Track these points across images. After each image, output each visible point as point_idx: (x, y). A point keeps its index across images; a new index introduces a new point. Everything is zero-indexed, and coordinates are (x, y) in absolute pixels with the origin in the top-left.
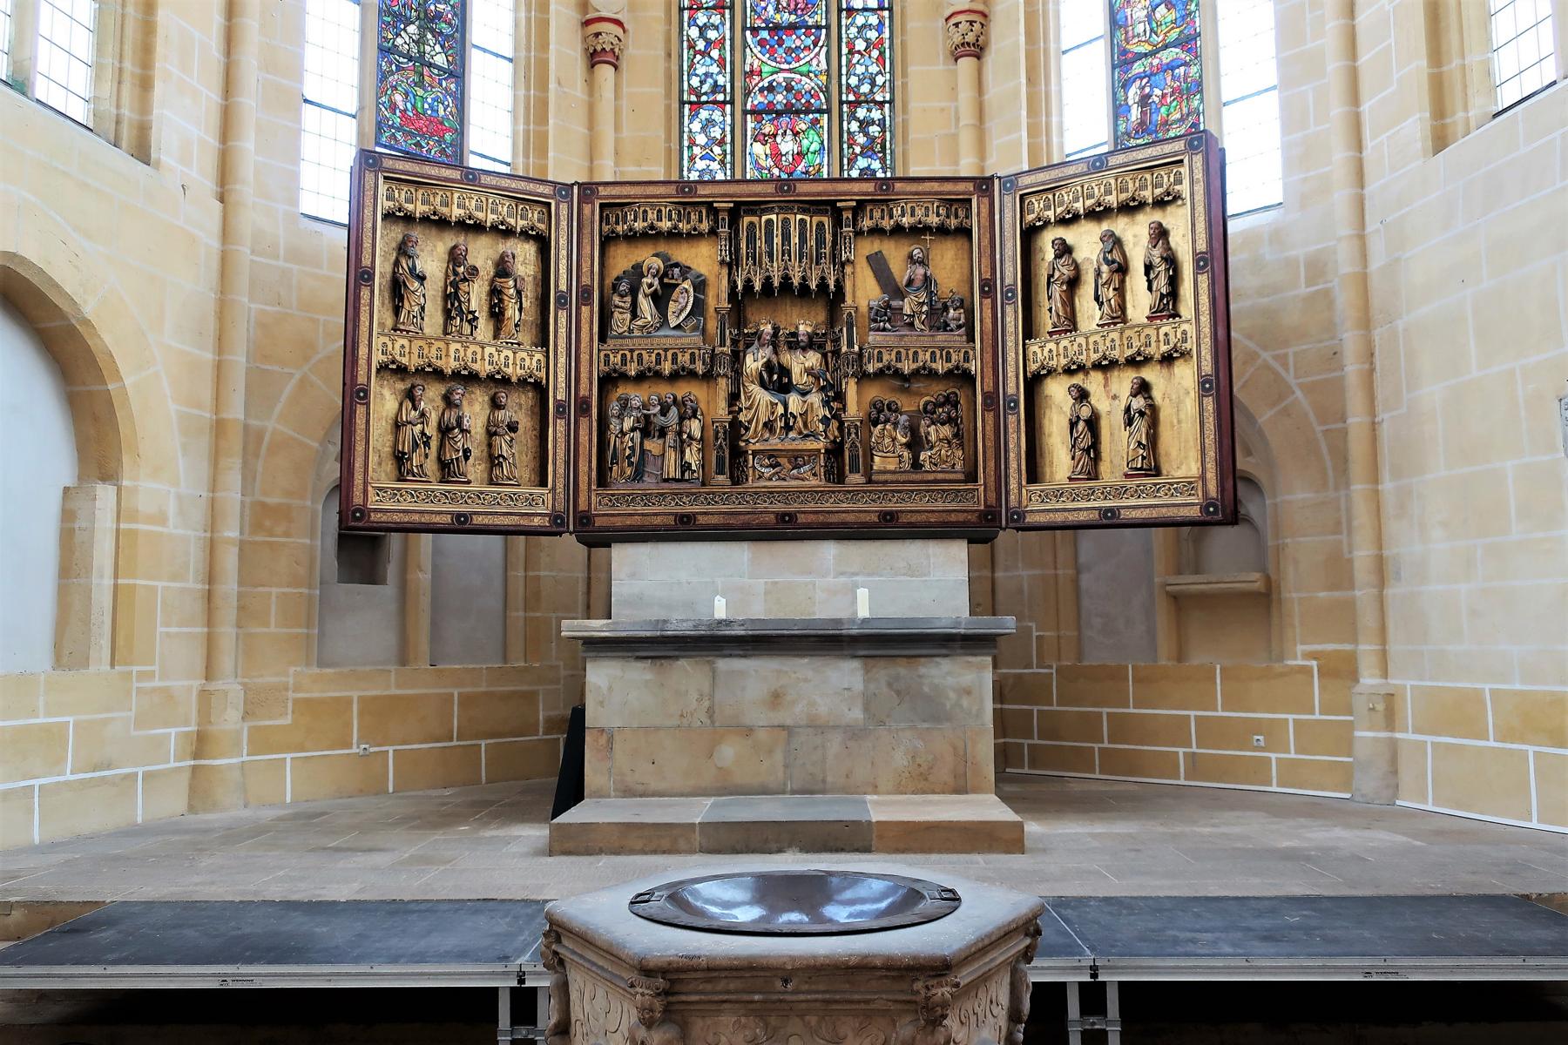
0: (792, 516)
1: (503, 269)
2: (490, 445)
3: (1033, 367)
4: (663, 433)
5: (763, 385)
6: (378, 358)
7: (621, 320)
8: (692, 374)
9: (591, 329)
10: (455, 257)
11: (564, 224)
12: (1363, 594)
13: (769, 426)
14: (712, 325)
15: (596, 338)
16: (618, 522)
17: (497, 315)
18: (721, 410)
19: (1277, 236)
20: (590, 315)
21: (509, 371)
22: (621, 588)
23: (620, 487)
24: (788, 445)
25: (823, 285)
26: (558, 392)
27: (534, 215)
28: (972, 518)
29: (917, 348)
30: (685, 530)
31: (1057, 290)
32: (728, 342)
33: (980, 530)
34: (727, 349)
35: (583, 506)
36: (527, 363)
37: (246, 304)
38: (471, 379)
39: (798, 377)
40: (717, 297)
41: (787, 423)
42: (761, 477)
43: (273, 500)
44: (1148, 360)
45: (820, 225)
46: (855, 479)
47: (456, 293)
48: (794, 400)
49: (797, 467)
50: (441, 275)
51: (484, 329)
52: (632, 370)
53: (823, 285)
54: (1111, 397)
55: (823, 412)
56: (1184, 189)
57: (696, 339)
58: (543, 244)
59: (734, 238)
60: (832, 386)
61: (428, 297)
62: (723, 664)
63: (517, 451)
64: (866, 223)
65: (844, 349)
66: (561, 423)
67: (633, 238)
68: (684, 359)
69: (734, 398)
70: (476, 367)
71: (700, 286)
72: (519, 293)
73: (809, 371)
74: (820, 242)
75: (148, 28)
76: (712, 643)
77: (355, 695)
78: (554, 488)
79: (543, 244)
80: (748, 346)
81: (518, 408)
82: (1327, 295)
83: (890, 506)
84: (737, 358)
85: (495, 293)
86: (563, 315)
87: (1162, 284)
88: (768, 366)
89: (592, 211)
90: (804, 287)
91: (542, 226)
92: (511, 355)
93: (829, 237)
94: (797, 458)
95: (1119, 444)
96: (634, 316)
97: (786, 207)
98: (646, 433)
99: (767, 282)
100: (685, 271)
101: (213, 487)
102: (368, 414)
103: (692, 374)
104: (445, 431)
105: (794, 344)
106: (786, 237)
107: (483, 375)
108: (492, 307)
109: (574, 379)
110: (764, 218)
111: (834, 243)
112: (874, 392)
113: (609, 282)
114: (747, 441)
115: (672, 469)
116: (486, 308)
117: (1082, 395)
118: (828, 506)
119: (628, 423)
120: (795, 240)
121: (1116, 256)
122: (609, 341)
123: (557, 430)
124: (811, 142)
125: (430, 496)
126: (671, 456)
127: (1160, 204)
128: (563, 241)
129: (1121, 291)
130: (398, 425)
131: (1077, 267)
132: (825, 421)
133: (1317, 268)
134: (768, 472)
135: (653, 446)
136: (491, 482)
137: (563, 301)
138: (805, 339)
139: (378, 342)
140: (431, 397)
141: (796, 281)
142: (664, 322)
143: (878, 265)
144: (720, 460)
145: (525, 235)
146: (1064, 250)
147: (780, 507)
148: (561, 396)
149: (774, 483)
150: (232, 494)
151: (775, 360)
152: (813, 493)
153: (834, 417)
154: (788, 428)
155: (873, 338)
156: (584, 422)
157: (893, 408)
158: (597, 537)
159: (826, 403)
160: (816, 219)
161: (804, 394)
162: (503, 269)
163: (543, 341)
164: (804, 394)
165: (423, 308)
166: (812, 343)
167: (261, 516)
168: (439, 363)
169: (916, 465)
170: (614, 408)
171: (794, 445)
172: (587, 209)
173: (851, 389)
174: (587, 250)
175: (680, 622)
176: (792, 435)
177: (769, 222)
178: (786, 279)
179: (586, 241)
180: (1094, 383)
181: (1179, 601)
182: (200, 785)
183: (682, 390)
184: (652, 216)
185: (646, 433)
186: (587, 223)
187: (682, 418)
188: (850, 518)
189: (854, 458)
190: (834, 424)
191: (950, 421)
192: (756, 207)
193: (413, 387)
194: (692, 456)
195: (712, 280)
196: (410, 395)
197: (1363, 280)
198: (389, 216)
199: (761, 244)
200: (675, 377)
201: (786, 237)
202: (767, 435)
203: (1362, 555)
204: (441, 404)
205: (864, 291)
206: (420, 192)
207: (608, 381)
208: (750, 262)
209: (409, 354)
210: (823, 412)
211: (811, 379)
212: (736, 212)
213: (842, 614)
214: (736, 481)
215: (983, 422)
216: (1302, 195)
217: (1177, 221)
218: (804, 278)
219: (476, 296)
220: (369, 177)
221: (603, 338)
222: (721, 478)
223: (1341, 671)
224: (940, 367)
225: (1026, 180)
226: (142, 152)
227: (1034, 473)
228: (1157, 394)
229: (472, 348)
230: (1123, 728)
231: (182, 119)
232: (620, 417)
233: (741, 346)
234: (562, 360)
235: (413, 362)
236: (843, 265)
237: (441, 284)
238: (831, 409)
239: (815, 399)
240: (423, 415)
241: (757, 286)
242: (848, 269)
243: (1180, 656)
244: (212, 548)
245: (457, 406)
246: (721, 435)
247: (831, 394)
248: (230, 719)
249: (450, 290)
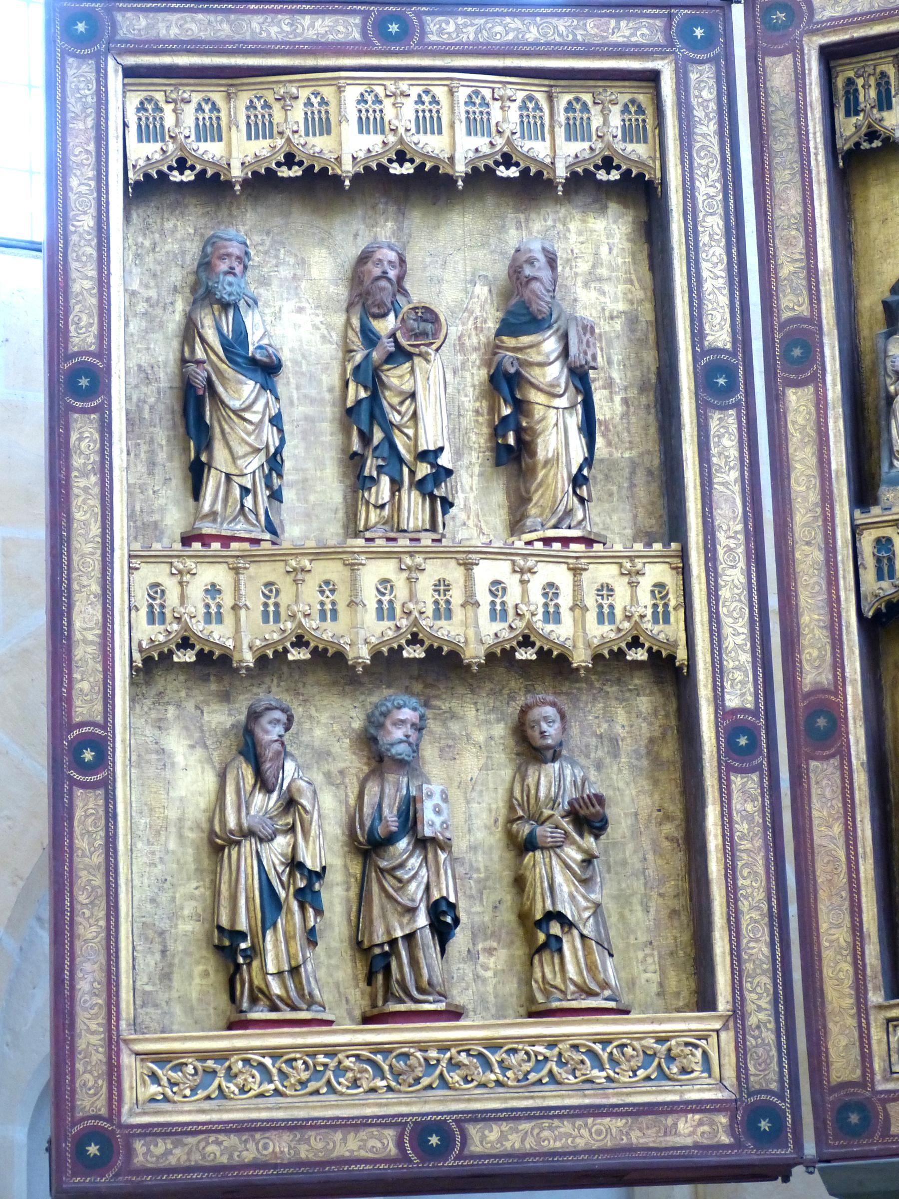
1: (522, 314)
2: (519, 883)
9: (823, 461)
10: (369, 291)
11: (707, 130)
15: (842, 489)
21: (562, 632)
26: (729, 683)
27: (609, 119)
36: (621, 598)
38: (441, 667)
47: (375, 398)
50: (330, 351)
51: (477, 501)
63: (616, 902)
66: (746, 788)
70: (449, 631)
72: (580, 377)
78: (738, 1013)
79: (641, 194)
81: (609, 750)
85: (506, 384)
86: (725, 429)
91: (639, 151)
92: (561, 575)
102: (111, 816)
107: (474, 653)
108: (498, 429)
113: (871, 301)
116: (478, 437)
122: (887, 494)
123: (735, 810)
128: (708, 188)
137: (722, 379)
145: (584, 186)
148: (740, 695)
156: (823, 777)
165: (275, 462)
168: (328, 632)
172: (779, 73)
174: (788, 204)
179: (784, 177)
186: (781, 116)
193: (254, 716)
204: (349, 761)
206: (244, 99)
219: (441, 404)
221: (864, 493)
229: (434, 570)
234: (734, 576)
237: (337, 382)
240: (290, 803)
245: (401, 764)
249: (356, 393)
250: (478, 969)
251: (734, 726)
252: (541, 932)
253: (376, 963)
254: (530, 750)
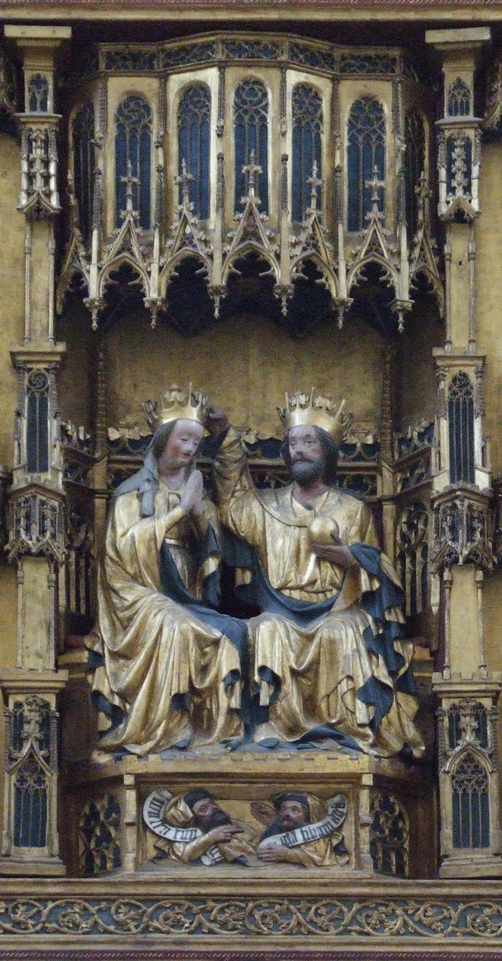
5: (170, 586)
13: (190, 705)
24: (250, 762)
25: (373, 279)
32: (55, 457)
34: (55, 479)
41: (250, 699)
42: (159, 848)
48: (273, 640)
49: (285, 826)
55: (367, 669)
59: (74, 145)
60: (398, 592)
65: (441, 482)
73: (324, 549)
80: (118, 478)
93: (393, 143)
94: (280, 801)
99: (188, 275)
105: (274, 469)
106: (250, 137)
110: (177, 82)
111: (412, 162)
114: (120, 751)
120: (281, 145)
132: (375, 693)
134: (186, 840)
138: (312, 451)
141: (284, 274)
149: (206, 871)
151: (209, 515)
153: (404, 684)
154: (252, 712)
159: (378, 644)
160: (351, 90)
161: (305, 614)
164: (305, 614)
171: (272, 764)
176: (263, 733)
177: (196, 95)
178: (251, 266)
190: (406, 705)
199: (165, 159)
201: (250, 137)
202: (183, 734)
208: (130, 213)
210: (367, 669)
211: (329, 572)
218: (310, 267)
222: (32, 853)
233: (99, 477)
236: (439, 229)
238: (394, 662)
239: (345, 634)
241: (154, 288)
242: (457, 245)
246: (31, 729)
247: (395, 617)
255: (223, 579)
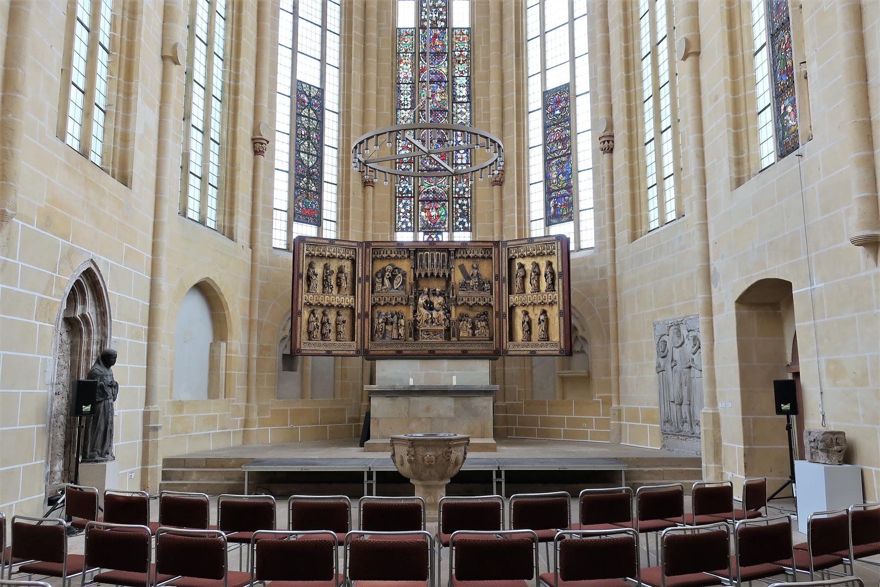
0: (433, 351)
3: (511, 304)
4: (392, 323)
5: (425, 308)
6: (304, 301)
7: (378, 286)
8: (402, 304)
10: (326, 267)
12: (613, 378)
13: (426, 321)
14: (408, 288)
16: (377, 353)
17: (339, 285)
18: (411, 317)
19: (592, 260)
20: (369, 285)
22: (379, 374)
23: (378, 341)
25: (444, 275)
26: (358, 310)
28: (492, 352)
29: (475, 296)
30: (399, 356)
31: (519, 280)
33: (495, 355)
35: (366, 347)
37: (259, 281)
39: (436, 305)
40: (410, 279)
42: (424, 338)
43: (265, 345)
44: (545, 304)
45: (444, 256)
46: (454, 339)
52: (382, 303)
53: (444, 275)
54: (535, 314)
56: (555, 251)
57: (403, 293)
58: (354, 262)
61: (318, 282)
62: (412, 399)
63: (345, 329)
64: (458, 255)
67: (382, 258)
68: (399, 300)
69: (415, 312)
71: (404, 275)
73: (439, 304)
74: (443, 261)
75: (232, 196)
76: (409, 392)
77: (289, 409)
79: (354, 262)
82: (605, 281)
83: (466, 348)
84: (416, 299)
85: (338, 278)
86: (360, 285)
87: (549, 280)
88: (426, 302)
89: (369, 251)
90: (438, 276)
94: (435, 332)
95: (537, 330)
96: (383, 285)
97: (432, 250)
98: (386, 324)
100: (399, 270)
101: (249, 340)
103: (402, 304)
104: (323, 324)
109: (363, 306)
112: (461, 310)
115: (395, 336)
117: (526, 313)
118: (445, 348)
119: (381, 320)
120: (435, 261)
121: (536, 270)
123: (358, 323)
124: (442, 212)
125: (320, 345)
126: (395, 331)
127: (549, 254)
129: (538, 281)
130: (309, 322)
131: (525, 271)
132: (444, 320)
133: (603, 272)
135: (389, 328)
136: (337, 340)
139: (304, 296)
140: (319, 312)
142: (393, 287)
143: (462, 268)
144: (410, 333)
146: (522, 266)
147: (430, 348)
150: (255, 344)
152: (441, 344)
154: (432, 322)
155: (460, 293)
156: (366, 320)
157: (467, 316)
158: (371, 357)
159: (445, 314)
162: (341, 270)
163: (353, 293)
166: (441, 294)
167: (262, 350)
169: (474, 335)
170: (376, 315)
173: (453, 309)
175: (399, 386)
180: (530, 310)
181: (563, 379)
182: (246, 435)
183: (398, 309)
184: (389, 252)
185: (386, 324)
187: (398, 319)
188: (452, 352)
189: (454, 333)
191: (485, 320)
192: (422, 250)
194: (401, 331)
195: (408, 273)
196: (313, 312)
197: (614, 278)
198: (307, 256)
200: (396, 304)
203: (613, 365)
205: (458, 277)
207: (374, 306)
209: (311, 298)
212: (416, 251)
213: (448, 384)
214: (415, 339)
215: (495, 321)
216: (599, 247)
217: (554, 260)
219: (333, 280)
220: (302, 244)
221: (373, 292)
223: (607, 402)
224: (481, 303)
225: (510, 243)
226: (231, 237)
227: (511, 338)
228: (548, 314)
230: (544, 421)
231: (242, 226)
232: (378, 318)
235: (314, 302)
239: (441, 313)
243: (563, 398)
244: (249, 361)
248: (254, 416)
250: (332, 336)
251: (359, 315)
252: (338, 333)
253: (323, 335)
254: (338, 314)
255: (429, 306)
